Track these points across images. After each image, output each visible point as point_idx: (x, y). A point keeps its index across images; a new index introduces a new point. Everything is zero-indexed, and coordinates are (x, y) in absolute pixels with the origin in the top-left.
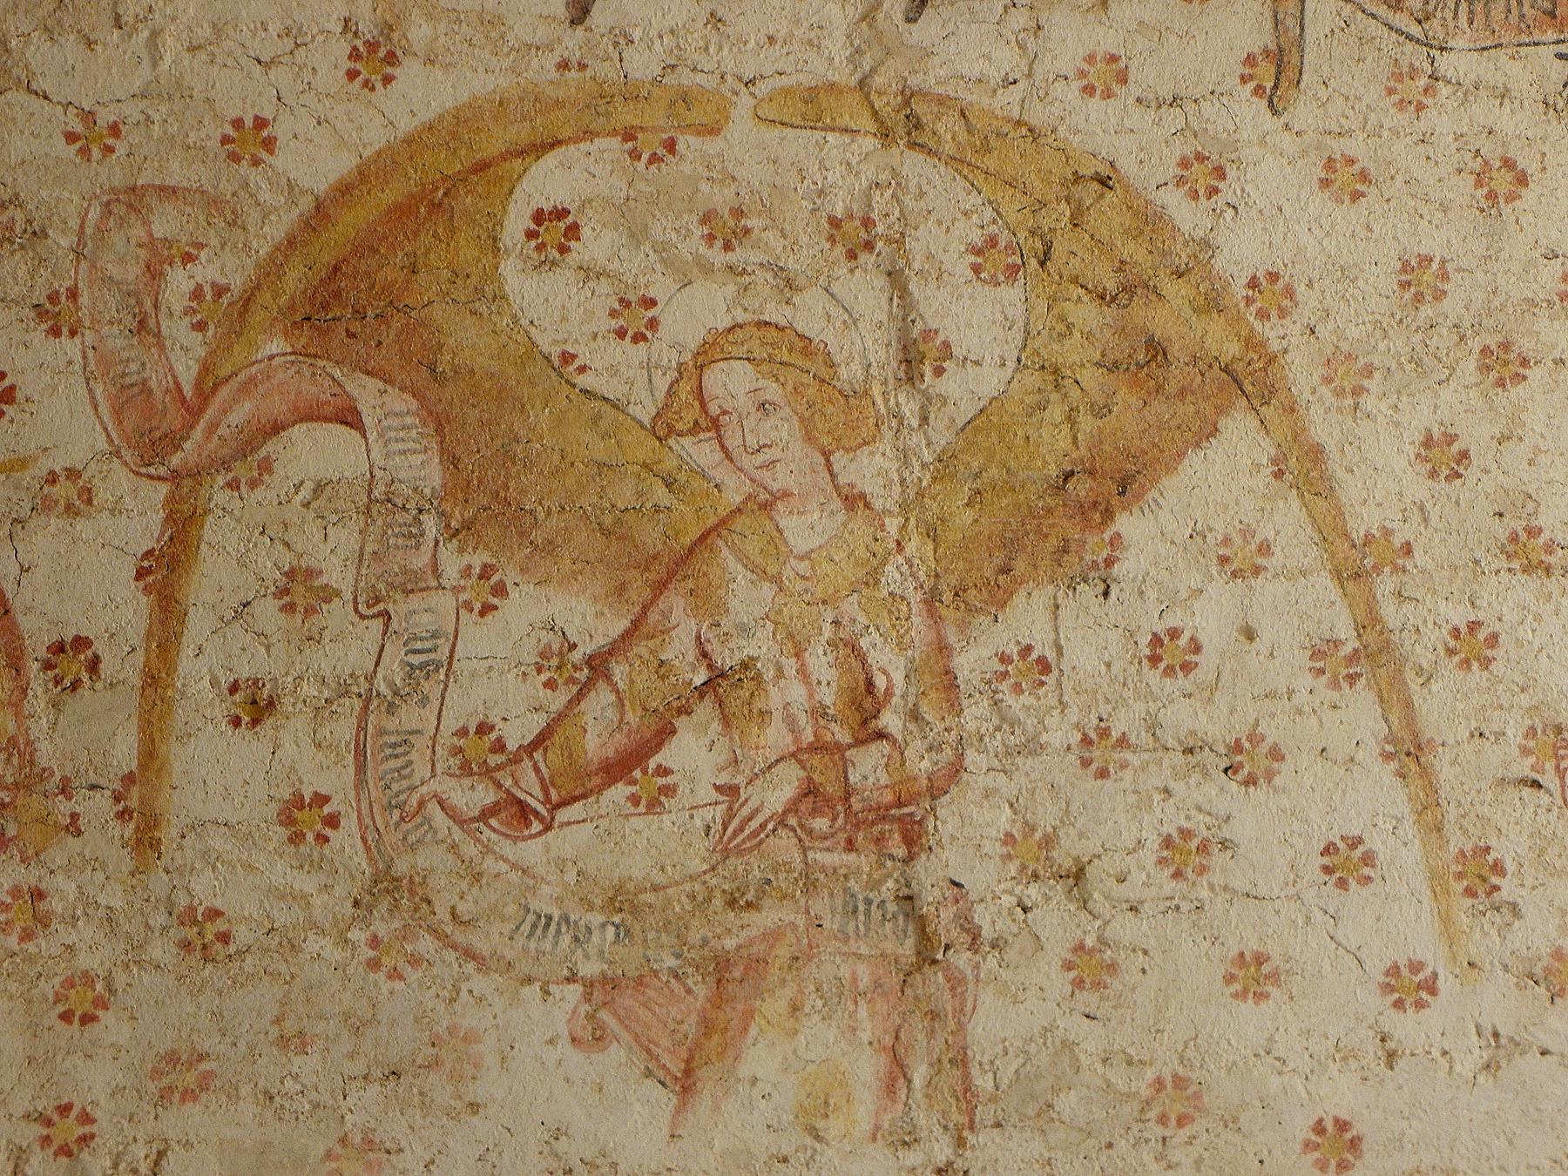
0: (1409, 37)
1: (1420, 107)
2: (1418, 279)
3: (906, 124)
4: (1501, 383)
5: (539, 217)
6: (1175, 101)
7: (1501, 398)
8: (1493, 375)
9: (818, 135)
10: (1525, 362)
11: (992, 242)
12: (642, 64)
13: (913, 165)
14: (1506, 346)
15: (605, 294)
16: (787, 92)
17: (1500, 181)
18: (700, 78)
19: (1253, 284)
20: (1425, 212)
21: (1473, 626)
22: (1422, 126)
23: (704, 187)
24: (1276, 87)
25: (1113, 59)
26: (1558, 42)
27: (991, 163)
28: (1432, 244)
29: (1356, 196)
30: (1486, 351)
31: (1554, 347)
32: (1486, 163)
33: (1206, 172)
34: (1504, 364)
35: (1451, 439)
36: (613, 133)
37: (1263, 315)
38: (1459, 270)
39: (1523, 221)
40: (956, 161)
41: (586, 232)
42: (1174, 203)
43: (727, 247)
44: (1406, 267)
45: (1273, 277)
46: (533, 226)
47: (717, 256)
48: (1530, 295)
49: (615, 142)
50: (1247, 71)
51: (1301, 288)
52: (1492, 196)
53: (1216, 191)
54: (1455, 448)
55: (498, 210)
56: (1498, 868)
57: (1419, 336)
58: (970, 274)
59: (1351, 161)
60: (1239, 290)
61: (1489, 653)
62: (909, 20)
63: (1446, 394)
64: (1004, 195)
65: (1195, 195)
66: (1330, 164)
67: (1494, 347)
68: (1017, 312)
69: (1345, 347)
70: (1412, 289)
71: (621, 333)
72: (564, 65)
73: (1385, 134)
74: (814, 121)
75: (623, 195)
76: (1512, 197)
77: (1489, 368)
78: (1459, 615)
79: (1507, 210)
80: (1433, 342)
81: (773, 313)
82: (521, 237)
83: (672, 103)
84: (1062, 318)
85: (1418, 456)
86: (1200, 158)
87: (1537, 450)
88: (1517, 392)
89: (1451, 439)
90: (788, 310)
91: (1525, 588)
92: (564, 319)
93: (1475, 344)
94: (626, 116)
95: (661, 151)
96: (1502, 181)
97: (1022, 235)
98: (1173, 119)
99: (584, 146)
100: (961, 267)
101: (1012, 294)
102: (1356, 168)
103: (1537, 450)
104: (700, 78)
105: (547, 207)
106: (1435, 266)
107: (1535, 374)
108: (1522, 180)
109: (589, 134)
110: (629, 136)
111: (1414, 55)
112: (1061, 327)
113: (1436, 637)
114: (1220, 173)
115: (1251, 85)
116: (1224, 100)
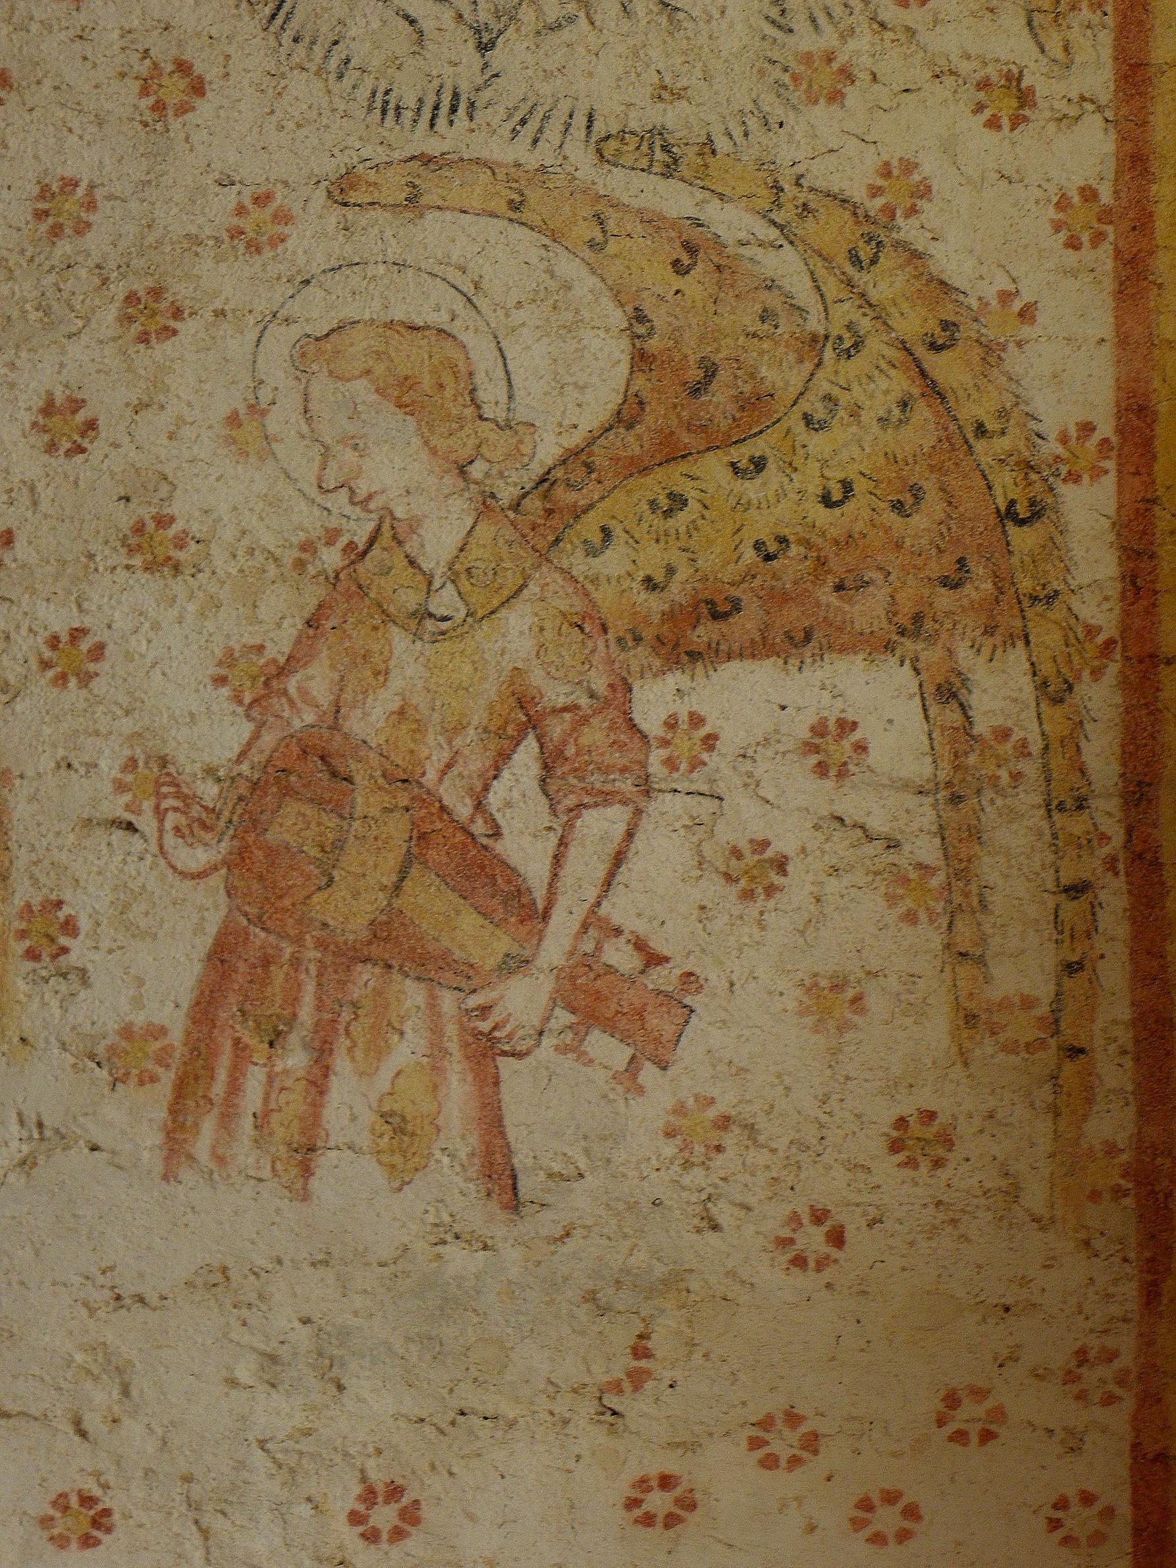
4: (144, 338)
7: (144, 358)
8: (136, 329)
10: (177, 313)
14: (157, 293)
20: (75, 124)
21: (77, 634)
22: (83, 19)
28: (81, 163)
30: (131, 298)
31: (216, 295)
32: (156, 66)
34: (151, 315)
35: (76, 405)
38: (110, 197)
39: (195, 138)
44: (45, 193)
48: (193, 230)
52: (159, 107)
54: (81, 416)
56: (70, 927)
57: (52, 278)
61: (92, 667)
63: (75, 350)
67: (141, 293)
70: (50, 220)
73: (34, 27)
76: (183, 109)
77: (131, 319)
78: (60, 620)
79: (175, 124)
80: (67, 287)
85: (34, 424)
87: (180, 421)
88: (164, 350)
89: (76, 405)
91: (144, 590)
93: (119, 290)
96: (173, 89)
103: (180, 421)
106: (81, 191)
107: (188, 328)
108: (198, 88)
113: (27, 645)
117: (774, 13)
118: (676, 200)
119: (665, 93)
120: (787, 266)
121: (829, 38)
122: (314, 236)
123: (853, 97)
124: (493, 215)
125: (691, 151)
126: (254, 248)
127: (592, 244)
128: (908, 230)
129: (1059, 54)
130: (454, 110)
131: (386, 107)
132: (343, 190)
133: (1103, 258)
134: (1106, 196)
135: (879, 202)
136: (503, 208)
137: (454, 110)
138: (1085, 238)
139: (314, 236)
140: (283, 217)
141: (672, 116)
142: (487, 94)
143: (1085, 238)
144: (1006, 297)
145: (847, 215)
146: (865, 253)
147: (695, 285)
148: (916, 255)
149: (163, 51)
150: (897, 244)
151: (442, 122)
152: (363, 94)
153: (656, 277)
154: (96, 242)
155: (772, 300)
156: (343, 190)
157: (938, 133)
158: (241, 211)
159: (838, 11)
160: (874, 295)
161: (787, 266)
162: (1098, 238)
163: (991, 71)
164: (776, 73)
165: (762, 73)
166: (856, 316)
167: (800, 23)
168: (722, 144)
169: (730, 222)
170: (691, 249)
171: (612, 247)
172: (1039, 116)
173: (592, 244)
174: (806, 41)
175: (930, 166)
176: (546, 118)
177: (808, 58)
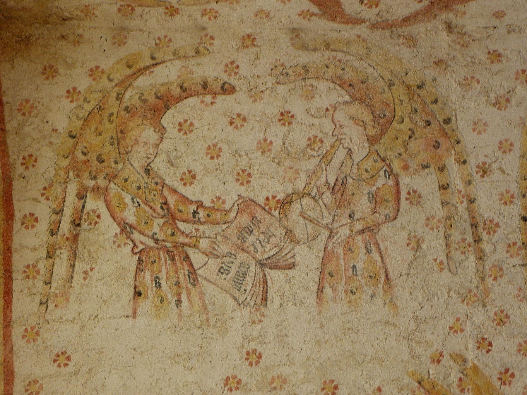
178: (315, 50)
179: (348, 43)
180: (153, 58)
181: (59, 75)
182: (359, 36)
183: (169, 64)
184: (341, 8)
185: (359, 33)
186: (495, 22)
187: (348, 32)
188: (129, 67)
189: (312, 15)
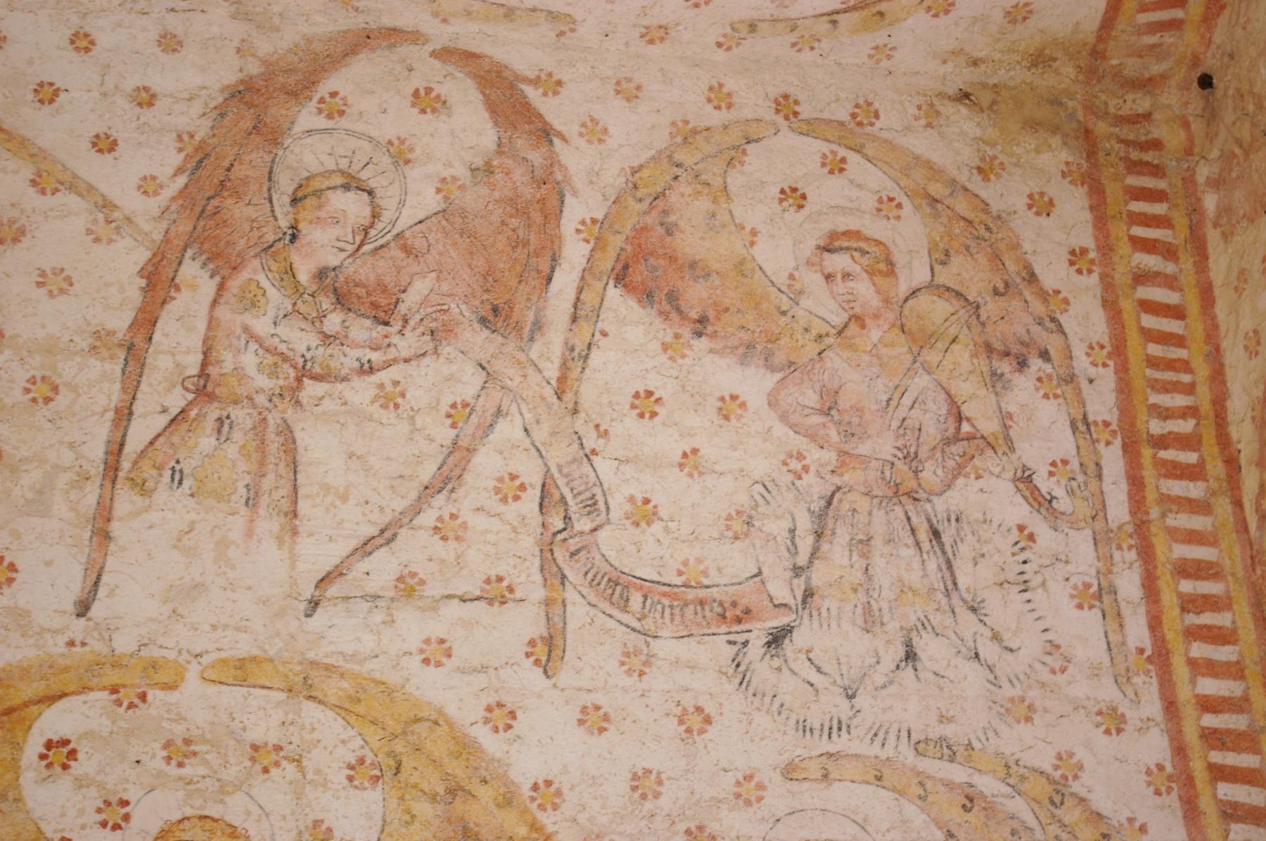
0: (633, 630)
1: (642, 674)
2: (643, 784)
3: (304, 685)
5: (49, 745)
6: (483, 669)
9: (245, 690)
11: (361, 761)
12: (124, 643)
13: (311, 711)
15: (93, 798)
16: (224, 662)
17: (693, 722)
18: (164, 652)
19: (535, 787)
23: (165, 724)
24: (548, 660)
25: (442, 641)
26: (729, 633)
27: (361, 709)
29: (602, 730)
32: (684, 709)
33: (503, 716)
36: (104, 688)
37: (542, 807)
38: (669, 778)
40: (338, 708)
41: (80, 756)
42: (483, 735)
43: (180, 765)
44: (635, 777)
45: (548, 783)
46: (45, 751)
47: (172, 770)
49: (104, 695)
50: (530, 650)
51: (565, 791)
52: (689, 731)
53: (509, 727)
55: (20, 740)
57: (644, 822)
58: (346, 782)
59: (597, 708)
60: (526, 791)
62: (307, 616)
64: (370, 730)
65: (496, 730)
66: (584, 710)
67: (693, 829)
68: (377, 810)
69: (596, 830)
70: (640, 791)
71: (104, 824)
72: (71, 643)
74: (242, 682)
75: (109, 730)
76: (702, 732)
81: (213, 811)
82: (35, 758)
83: (145, 669)
84: (408, 811)
86: (500, 705)
90: (220, 807)
92: (63, 815)
94: (112, 677)
95: (136, 701)
96: (695, 721)
97: (381, 756)
98: (481, 680)
99: (82, 698)
100: (340, 777)
101: (373, 796)
102: (601, 712)
104: (164, 652)
105: (55, 738)
108: (708, 720)
109: (86, 689)
110: (114, 690)
111: (635, 640)
112: (407, 817)
114: (512, 715)
115: (532, 659)
116: (515, 667)
117: (991, 677)
118: (959, 774)
119: (943, 719)
120: (1018, 806)
121: (1016, 692)
122: (778, 797)
123: (1036, 718)
124: (868, 783)
125: (962, 748)
126: (748, 803)
127: (920, 797)
128: (1076, 787)
129: (1133, 697)
130: (840, 729)
131: (804, 728)
132: (790, 772)
133: (1173, 800)
134: (1169, 769)
135: (1060, 772)
136: (872, 780)
137: (840, 729)
138: (1163, 789)
139: (778, 797)
140: (761, 786)
141: (948, 730)
142: (855, 722)
143: (1163, 789)
144: (1131, 820)
145: (1044, 780)
146: (1057, 799)
147: (975, 817)
148: (1082, 800)
149: (688, 701)
150: (1072, 794)
151: (834, 735)
152: (792, 722)
153: (955, 815)
154: (665, 802)
155: (1015, 824)
156: (790, 772)
157: (1079, 735)
158: (738, 783)
159: (1022, 677)
160: (1066, 820)
161: (1018, 806)
162: (1169, 790)
163: (1102, 704)
164: (997, 708)
165: (990, 708)
166: (1059, 832)
167: (1006, 685)
168: (976, 744)
169: (988, 784)
170: (970, 801)
171: (931, 798)
172: (1129, 728)
173: (920, 797)
174: (1008, 691)
175: (1081, 754)
176: (887, 732)
177: (1012, 700)
178: (534, 10)
179: (468, 14)
180: (834, 22)
181: (1004, 9)
182: (445, 21)
183: (810, 13)
184: (484, 94)
185: (442, 26)
186: (174, 23)
187: (469, 35)
188: (881, 14)
189: (536, 82)
